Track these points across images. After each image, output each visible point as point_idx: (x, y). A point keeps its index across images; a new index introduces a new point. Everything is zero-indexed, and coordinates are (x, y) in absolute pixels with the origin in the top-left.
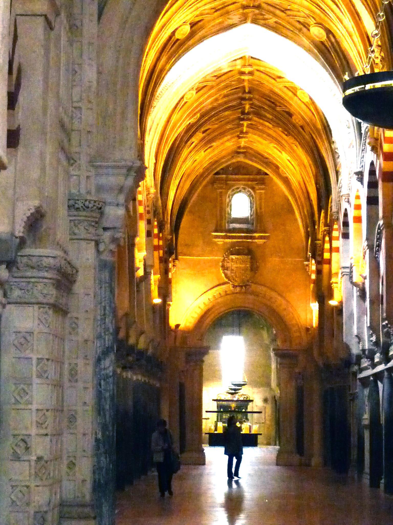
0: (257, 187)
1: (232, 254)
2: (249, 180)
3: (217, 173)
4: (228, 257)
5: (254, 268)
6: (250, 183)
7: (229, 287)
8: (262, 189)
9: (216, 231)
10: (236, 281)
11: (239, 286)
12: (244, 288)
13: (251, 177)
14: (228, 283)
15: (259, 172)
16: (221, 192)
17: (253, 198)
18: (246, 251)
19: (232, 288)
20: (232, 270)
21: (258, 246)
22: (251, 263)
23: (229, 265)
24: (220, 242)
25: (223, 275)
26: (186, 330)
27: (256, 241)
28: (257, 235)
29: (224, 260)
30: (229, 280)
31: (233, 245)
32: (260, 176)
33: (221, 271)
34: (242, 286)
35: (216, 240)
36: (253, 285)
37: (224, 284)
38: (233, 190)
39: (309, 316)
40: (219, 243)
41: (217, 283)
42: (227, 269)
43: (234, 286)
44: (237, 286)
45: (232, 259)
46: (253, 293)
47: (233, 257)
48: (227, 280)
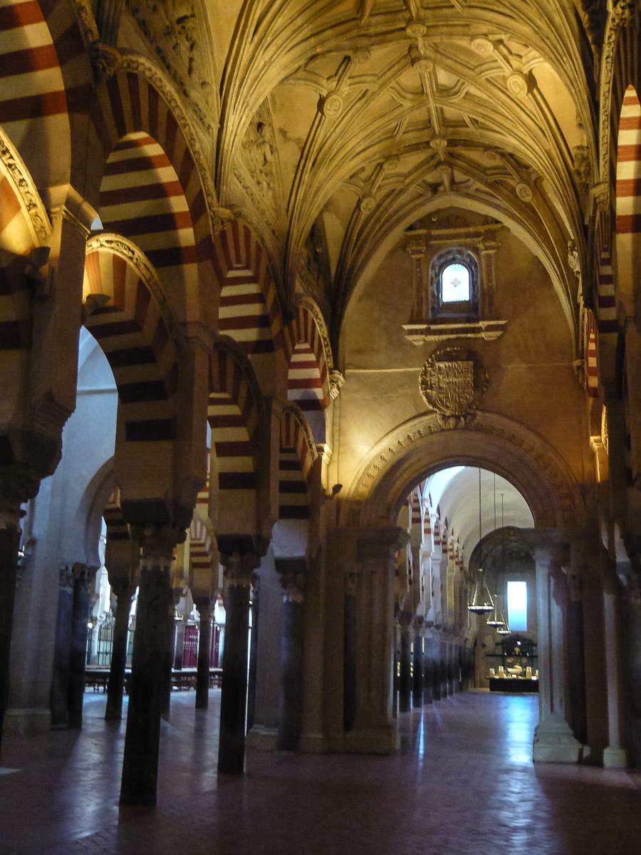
0: (481, 246)
1: (440, 360)
2: (467, 235)
3: (411, 228)
4: (432, 365)
5: (479, 384)
6: (469, 240)
7: (435, 419)
8: (493, 248)
9: (412, 322)
10: (447, 407)
11: (453, 416)
12: (462, 419)
13: (471, 230)
14: (432, 412)
15: (487, 220)
16: (418, 260)
17: (476, 266)
18: (465, 356)
19: (440, 422)
20: (440, 388)
21: (487, 343)
22: (475, 374)
23: (434, 380)
24: (418, 340)
25: (424, 398)
26: (357, 498)
27: (483, 335)
28: (482, 324)
29: (425, 373)
30: (434, 406)
31: (442, 345)
32: (488, 227)
33: (421, 392)
34: (458, 418)
35: (410, 338)
36: (479, 413)
37: (425, 414)
38: (440, 257)
39: (588, 465)
40: (416, 343)
41: (414, 413)
42: (431, 388)
43: (445, 418)
44: (449, 417)
45: (440, 368)
46: (480, 429)
47: (442, 365)
48: (431, 408)
